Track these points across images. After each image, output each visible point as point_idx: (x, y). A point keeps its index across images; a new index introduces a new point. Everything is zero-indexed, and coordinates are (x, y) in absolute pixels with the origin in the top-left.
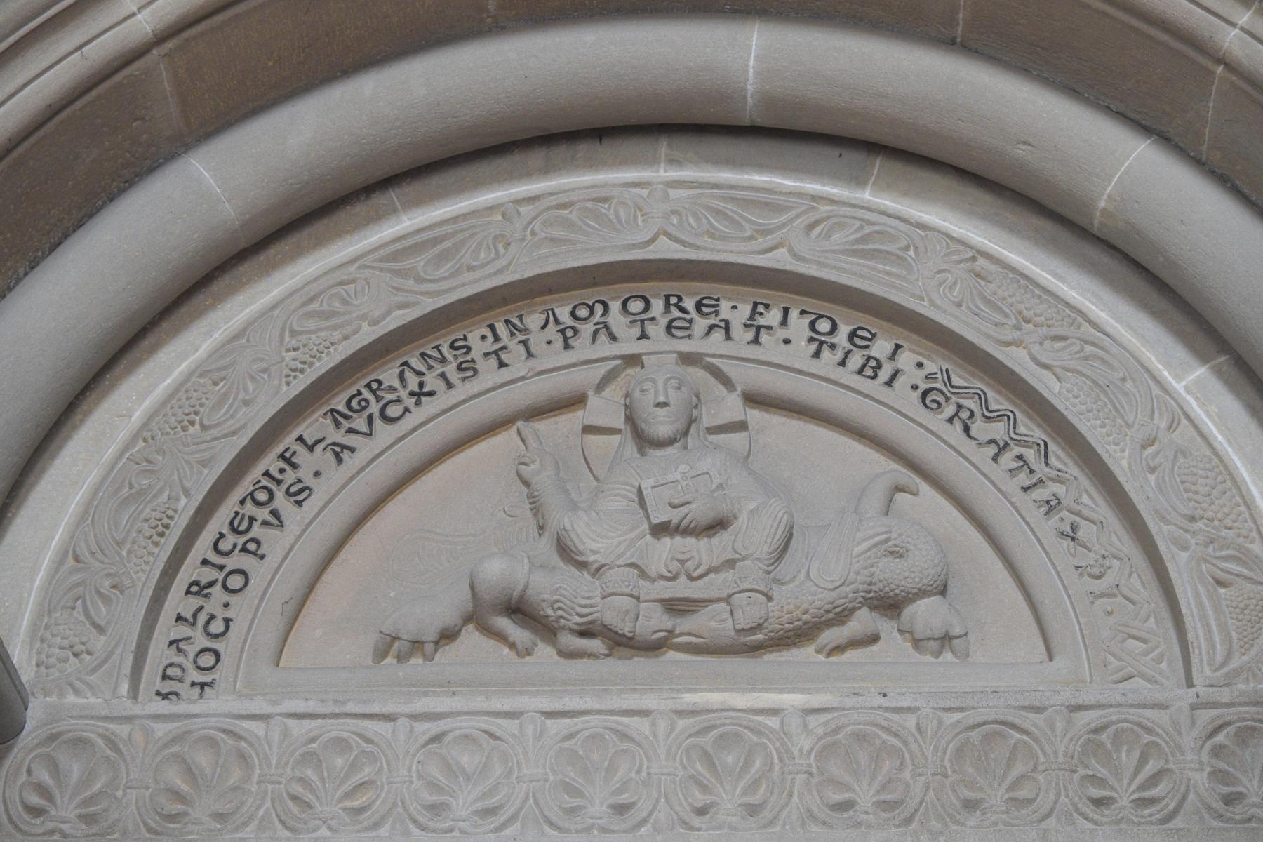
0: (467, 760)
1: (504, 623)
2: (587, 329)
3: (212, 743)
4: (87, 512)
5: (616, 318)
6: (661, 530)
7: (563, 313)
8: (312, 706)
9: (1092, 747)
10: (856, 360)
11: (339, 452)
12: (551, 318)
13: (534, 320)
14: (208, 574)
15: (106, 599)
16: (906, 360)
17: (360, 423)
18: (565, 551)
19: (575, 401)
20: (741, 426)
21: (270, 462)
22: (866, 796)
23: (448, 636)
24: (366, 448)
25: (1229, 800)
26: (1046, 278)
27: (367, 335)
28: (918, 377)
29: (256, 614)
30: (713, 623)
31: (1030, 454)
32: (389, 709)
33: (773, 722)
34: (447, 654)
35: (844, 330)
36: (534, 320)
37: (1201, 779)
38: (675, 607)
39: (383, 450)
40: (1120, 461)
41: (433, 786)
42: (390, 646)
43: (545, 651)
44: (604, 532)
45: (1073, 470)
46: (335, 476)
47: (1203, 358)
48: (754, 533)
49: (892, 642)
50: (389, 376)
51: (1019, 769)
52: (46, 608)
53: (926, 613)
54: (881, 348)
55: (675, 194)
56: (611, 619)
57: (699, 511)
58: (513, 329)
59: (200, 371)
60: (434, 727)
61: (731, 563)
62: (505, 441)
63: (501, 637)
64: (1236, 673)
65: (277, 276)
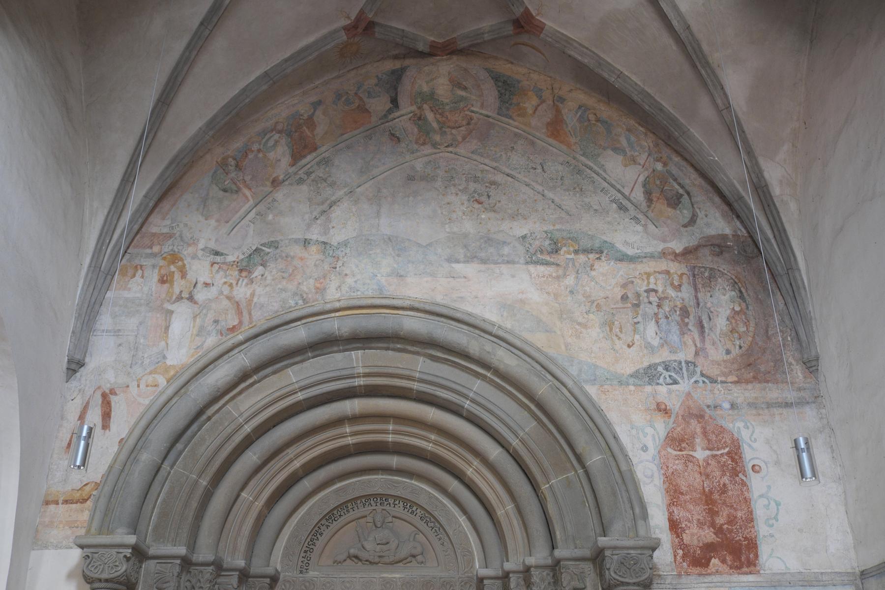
0: (348, 585)
5: (372, 502)
11: (328, 526)
16: (418, 511)
21: (317, 528)
24: (332, 526)
27: (332, 506)
29: (314, 556)
30: (386, 560)
34: (344, 564)
36: (359, 502)
38: (380, 557)
39: (335, 526)
40: (451, 533)
46: (327, 531)
48: (393, 545)
50: (335, 512)
52: (282, 558)
53: (419, 558)
54: (414, 508)
57: (384, 541)
59: (305, 513)
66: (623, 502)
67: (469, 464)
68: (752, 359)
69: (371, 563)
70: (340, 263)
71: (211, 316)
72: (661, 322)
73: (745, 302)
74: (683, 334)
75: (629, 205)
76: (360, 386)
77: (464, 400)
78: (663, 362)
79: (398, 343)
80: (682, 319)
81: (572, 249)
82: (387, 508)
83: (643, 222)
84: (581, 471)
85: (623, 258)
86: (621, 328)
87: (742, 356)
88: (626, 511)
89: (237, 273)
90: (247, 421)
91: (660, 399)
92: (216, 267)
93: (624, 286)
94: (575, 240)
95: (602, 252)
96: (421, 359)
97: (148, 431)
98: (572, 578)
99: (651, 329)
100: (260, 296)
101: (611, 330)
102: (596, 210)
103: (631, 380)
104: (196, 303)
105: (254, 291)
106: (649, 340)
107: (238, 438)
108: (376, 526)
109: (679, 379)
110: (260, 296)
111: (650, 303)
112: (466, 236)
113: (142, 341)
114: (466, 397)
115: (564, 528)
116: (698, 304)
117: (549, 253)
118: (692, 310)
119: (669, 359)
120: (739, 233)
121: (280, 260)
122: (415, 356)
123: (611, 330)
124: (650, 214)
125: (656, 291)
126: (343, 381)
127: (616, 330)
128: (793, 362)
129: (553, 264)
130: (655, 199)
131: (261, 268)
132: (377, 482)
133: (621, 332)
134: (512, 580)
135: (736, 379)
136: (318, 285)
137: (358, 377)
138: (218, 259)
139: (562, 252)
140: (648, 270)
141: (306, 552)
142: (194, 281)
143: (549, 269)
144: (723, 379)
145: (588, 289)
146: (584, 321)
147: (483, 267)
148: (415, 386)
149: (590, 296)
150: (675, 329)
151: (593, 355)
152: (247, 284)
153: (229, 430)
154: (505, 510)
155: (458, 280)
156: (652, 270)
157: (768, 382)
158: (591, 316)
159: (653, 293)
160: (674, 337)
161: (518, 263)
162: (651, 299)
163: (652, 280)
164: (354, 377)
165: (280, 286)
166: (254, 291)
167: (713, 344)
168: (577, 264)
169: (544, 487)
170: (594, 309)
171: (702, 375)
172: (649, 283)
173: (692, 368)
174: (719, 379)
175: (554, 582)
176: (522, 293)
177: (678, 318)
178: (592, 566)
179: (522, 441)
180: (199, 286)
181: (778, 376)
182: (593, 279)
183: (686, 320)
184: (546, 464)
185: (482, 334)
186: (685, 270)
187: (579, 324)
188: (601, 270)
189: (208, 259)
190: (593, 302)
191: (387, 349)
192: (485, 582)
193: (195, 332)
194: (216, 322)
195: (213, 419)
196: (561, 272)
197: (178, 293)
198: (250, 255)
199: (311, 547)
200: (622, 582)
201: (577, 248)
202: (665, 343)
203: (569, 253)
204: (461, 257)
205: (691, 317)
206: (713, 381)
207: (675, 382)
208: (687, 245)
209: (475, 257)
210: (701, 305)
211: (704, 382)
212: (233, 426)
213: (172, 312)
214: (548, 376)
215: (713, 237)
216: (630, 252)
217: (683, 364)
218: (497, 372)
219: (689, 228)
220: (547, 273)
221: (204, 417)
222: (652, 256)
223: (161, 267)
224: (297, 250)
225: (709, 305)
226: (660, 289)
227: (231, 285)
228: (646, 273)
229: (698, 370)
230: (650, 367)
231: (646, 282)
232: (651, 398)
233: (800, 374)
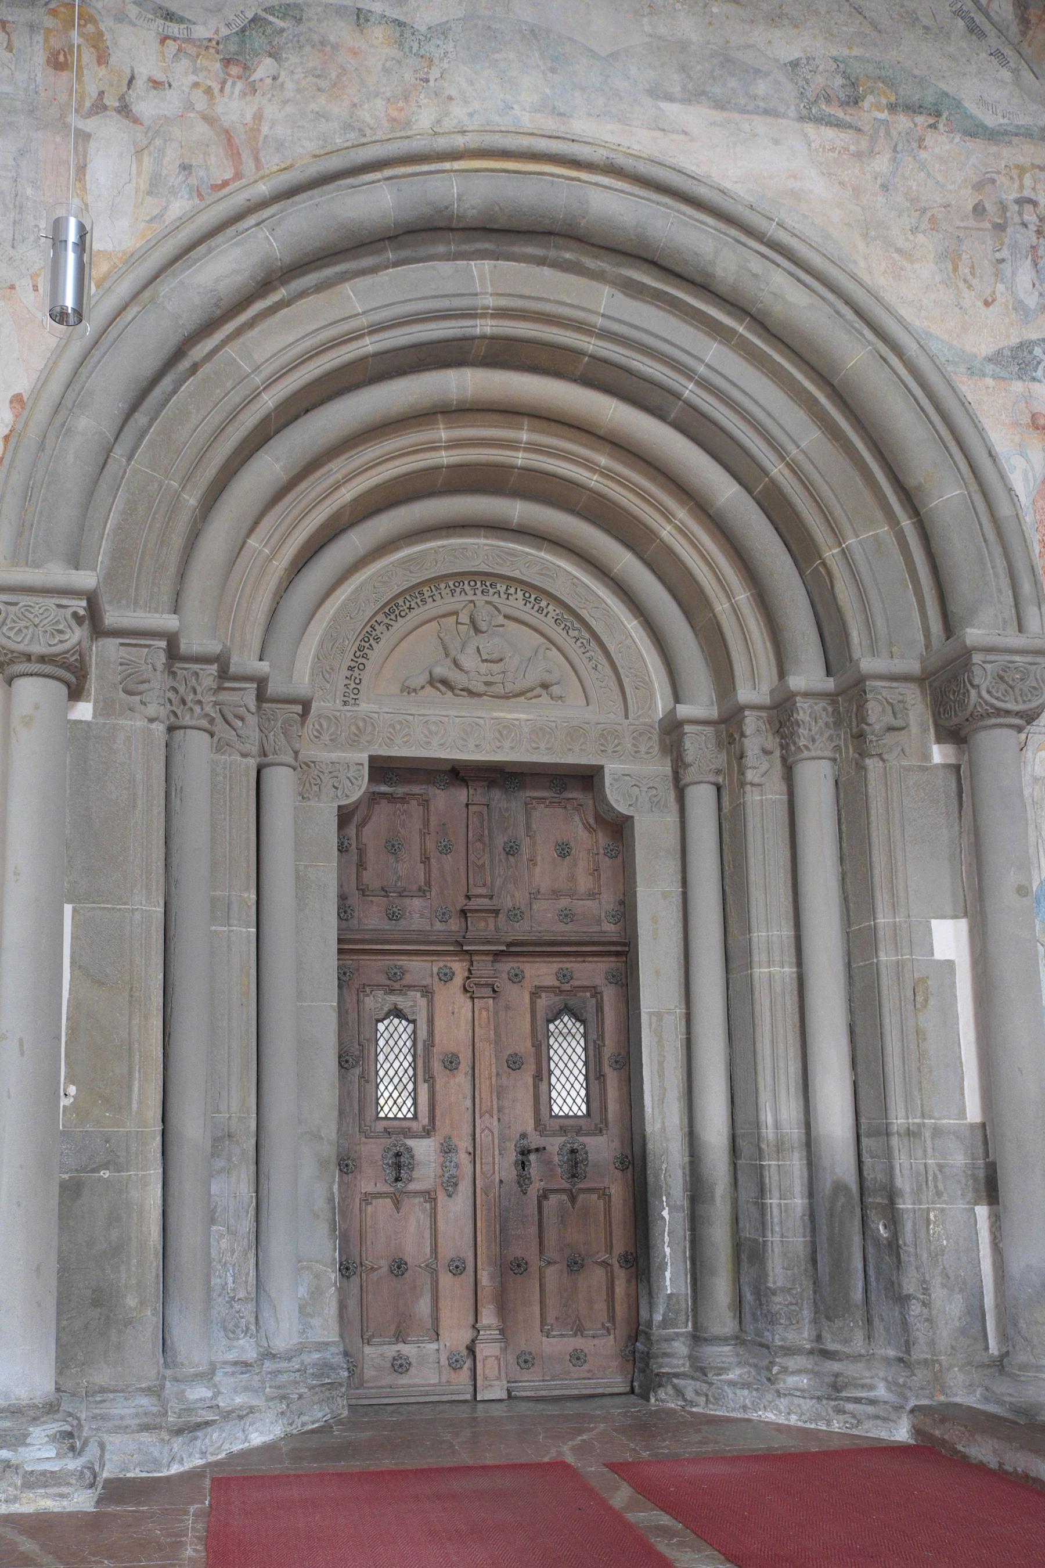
0: (433, 728)
1: (439, 685)
2: (458, 590)
3: (364, 720)
4: (321, 645)
5: (467, 587)
6: (484, 661)
7: (451, 584)
8: (391, 710)
9: (602, 735)
10: (536, 607)
11: (388, 626)
12: (447, 586)
13: (443, 586)
14: (353, 664)
15: (329, 673)
16: (551, 608)
17: (393, 617)
18: (456, 663)
19: (456, 613)
20: (503, 626)
22: (543, 746)
23: (423, 687)
24: (396, 626)
25: (636, 752)
26: (594, 588)
27: (397, 590)
28: (553, 614)
29: (366, 676)
30: (499, 689)
31: (585, 642)
32: (413, 712)
33: (517, 723)
34: (421, 693)
35: (533, 597)
37: (629, 746)
38: (487, 684)
39: (400, 626)
40: (611, 648)
41: (426, 736)
42: (408, 690)
43: (450, 693)
44: (469, 661)
45: (597, 648)
47: (636, 618)
49: (545, 698)
50: (400, 601)
51: (582, 740)
53: (555, 690)
54: (543, 604)
55: (486, 548)
56: (471, 687)
58: (437, 589)
59: (348, 599)
60: (426, 719)
61: (504, 672)
62: (434, 623)
63: (438, 689)
64: (639, 716)
65: (369, 567)
66: (996, 575)
67: (667, 515)
69: (471, 693)
70: (435, 73)
71: (172, 156)
75: (987, 27)
76: (483, 337)
77: (683, 380)
79: (567, 249)
81: (884, 101)
82: (495, 599)
83: (1011, 64)
84: (906, 524)
85: (976, 131)
86: (973, 267)
88: (1000, 591)
89: (218, 65)
90: (270, 383)
92: (172, 47)
94: (890, 83)
95: (939, 115)
96: (606, 290)
97: (84, 371)
98: (884, 711)
99: (1024, 275)
100: (273, 124)
101: (955, 270)
102: (926, 28)
103: (990, 368)
104: (136, 121)
105: (260, 110)
106: (1022, 296)
107: (250, 420)
108: (477, 630)
110: (273, 124)
111: (1025, 225)
112: (683, 46)
113: (29, 192)
114: (687, 373)
115: (869, 624)
117: (842, 104)
121: (308, 48)
122: (594, 284)
123: (955, 270)
124: (1027, 50)
126: (453, 323)
127: (964, 270)
130: (1034, 20)
131: (269, 61)
132: (479, 551)
133: (973, 274)
134: (747, 721)
136: (395, 114)
137: (483, 316)
138: (174, 29)
141: (351, 669)
142: (128, 72)
143: (842, 135)
147: (718, 116)
148: (591, 345)
151: (923, 313)
152: (243, 94)
153: (235, 398)
154: (731, 602)
155: (674, 136)
158: (921, 238)
159: (1029, 207)
161: (784, 116)
162: (1026, 218)
163: (1028, 181)
164: (474, 316)
165: (313, 106)
166: (260, 110)
168: (894, 133)
169: (831, 553)
170: (925, 225)
172: (1022, 186)
175: (835, 723)
176: (795, 178)
178: (918, 692)
179: (793, 468)
180: (140, 83)
182: (923, 166)
184: (838, 511)
185: (744, 238)
187: (899, 251)
188: (937, 150)
189: (153, 26)
190: (924, 211)
191: (541, 261)
192: (688, 728)
193: (143, 186)
194: (186, 168)
195: (201, 373)
196: (864, 145)
197: (95, 94)
198: (243, 30)
199: (360, 660)
200: (999, 710)
201: (893, 99)
203: (878, 107)
204: (676, 90)
209: (704, 93)
212: (243, 391)
213: (89, 136)
214: (867, 332)
216: (990, 121)
218: (761, 323)
221: (185, 364)
222: (1026, 134)
223: (48, 31)
224: (341, 31)
227: (209, 91)
228: (1017, 167)
230: (1021, 346)
231: (1016, 185)
232: (1023, 405)
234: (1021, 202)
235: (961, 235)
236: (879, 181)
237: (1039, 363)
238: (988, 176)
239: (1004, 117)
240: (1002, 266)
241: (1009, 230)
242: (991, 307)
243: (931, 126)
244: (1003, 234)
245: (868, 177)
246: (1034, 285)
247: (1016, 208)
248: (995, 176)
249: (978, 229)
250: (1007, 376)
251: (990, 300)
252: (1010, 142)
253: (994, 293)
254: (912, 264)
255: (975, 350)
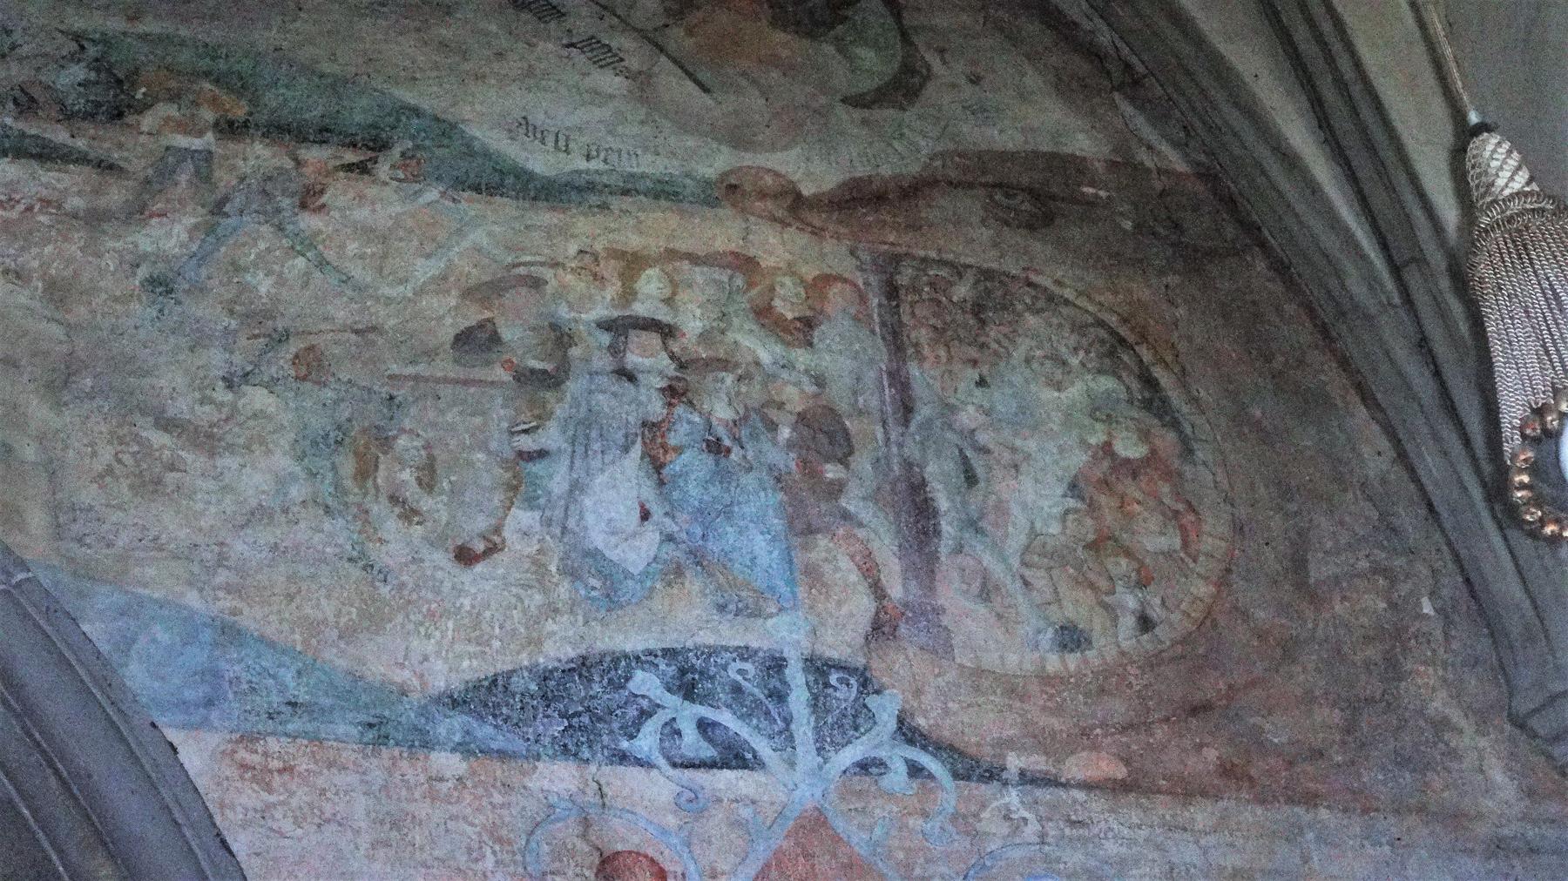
68: (1212, 686)
72: (676, 465)
73: (1175, 425)
74: (802, 529)
78: (669, 653)
80: (804, 463)
81: (208, 115)
87: (1153, 662)
91: (623, 835)
93: (486, 292)
94: (240, 85)
95: (380, 146)
101: (365, 473)
103: (451, 725)
109: (762, 747)
111: (628, 376)
116: (906, 409)
118: (866, 431)
119: (707, 638)
120: (1143, 156)
123: (365, 473)
125: (667, 332)
128: (1456, 716)
129: (82, 159)
133: (428, 482)
135: (1120, 772)
139: (148, 121)
140: (634, 242)
144: (1038, 763)
145: (265, 286)
146: (206, 414)
149: (268, 315)
150: (759, 503)
151: (222, 577)
156: (656, 245)
157: (1311, 800)
158: (257, 398)
159: (654, 339)
160: (755, 542)
162: (633, 359)
163: (651, 284)
167: (987, 591)
168: (224, 179)
171: (907, 732)
172: (628, 295)
173: (844, 694)
174: (1014, 762)
177: (788, 462)
181: (1370, 776)
182: (305, 244)
183: (832, 472)
186: (842, 264)
188: (362, 214)
190: (284, 337)
202: (689, 560)
205: (863, 462)
206: (974, 769)
207: (735, 757)
208: (861, 171)
210: (924, 412)
211: (915, 770)
215: (1005, 157)
216: (541, 162)
217: (796, 676)
219: (885, 115)
220: (31, 190)
225: (968, 417)
226: (692, 322)
229: (886, 709)
230: (583, 667)
231: (612, 290)
232: (567, 831)
233: (1498, 776)
234: (620, 328)
235: (401, 393)
236: (143, 272)
237: (645, 715)
238: (522, 270)
239: (588, 158)
240: (536, 468)
241: (573, 386)
242: (479, 568)
243: (349, 168)
244: (549, 395)
245: (110, 262)
246: (645, 515)
247: (606, 338)
248: (548, 273)
249: (466, 383)
250: (519, 745)
251: (480, 546)
252: (604, 207)
253: (497, 530)
254: (212, 454)
255: (402, 676)
